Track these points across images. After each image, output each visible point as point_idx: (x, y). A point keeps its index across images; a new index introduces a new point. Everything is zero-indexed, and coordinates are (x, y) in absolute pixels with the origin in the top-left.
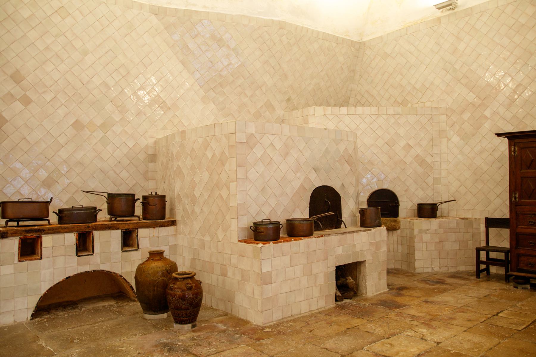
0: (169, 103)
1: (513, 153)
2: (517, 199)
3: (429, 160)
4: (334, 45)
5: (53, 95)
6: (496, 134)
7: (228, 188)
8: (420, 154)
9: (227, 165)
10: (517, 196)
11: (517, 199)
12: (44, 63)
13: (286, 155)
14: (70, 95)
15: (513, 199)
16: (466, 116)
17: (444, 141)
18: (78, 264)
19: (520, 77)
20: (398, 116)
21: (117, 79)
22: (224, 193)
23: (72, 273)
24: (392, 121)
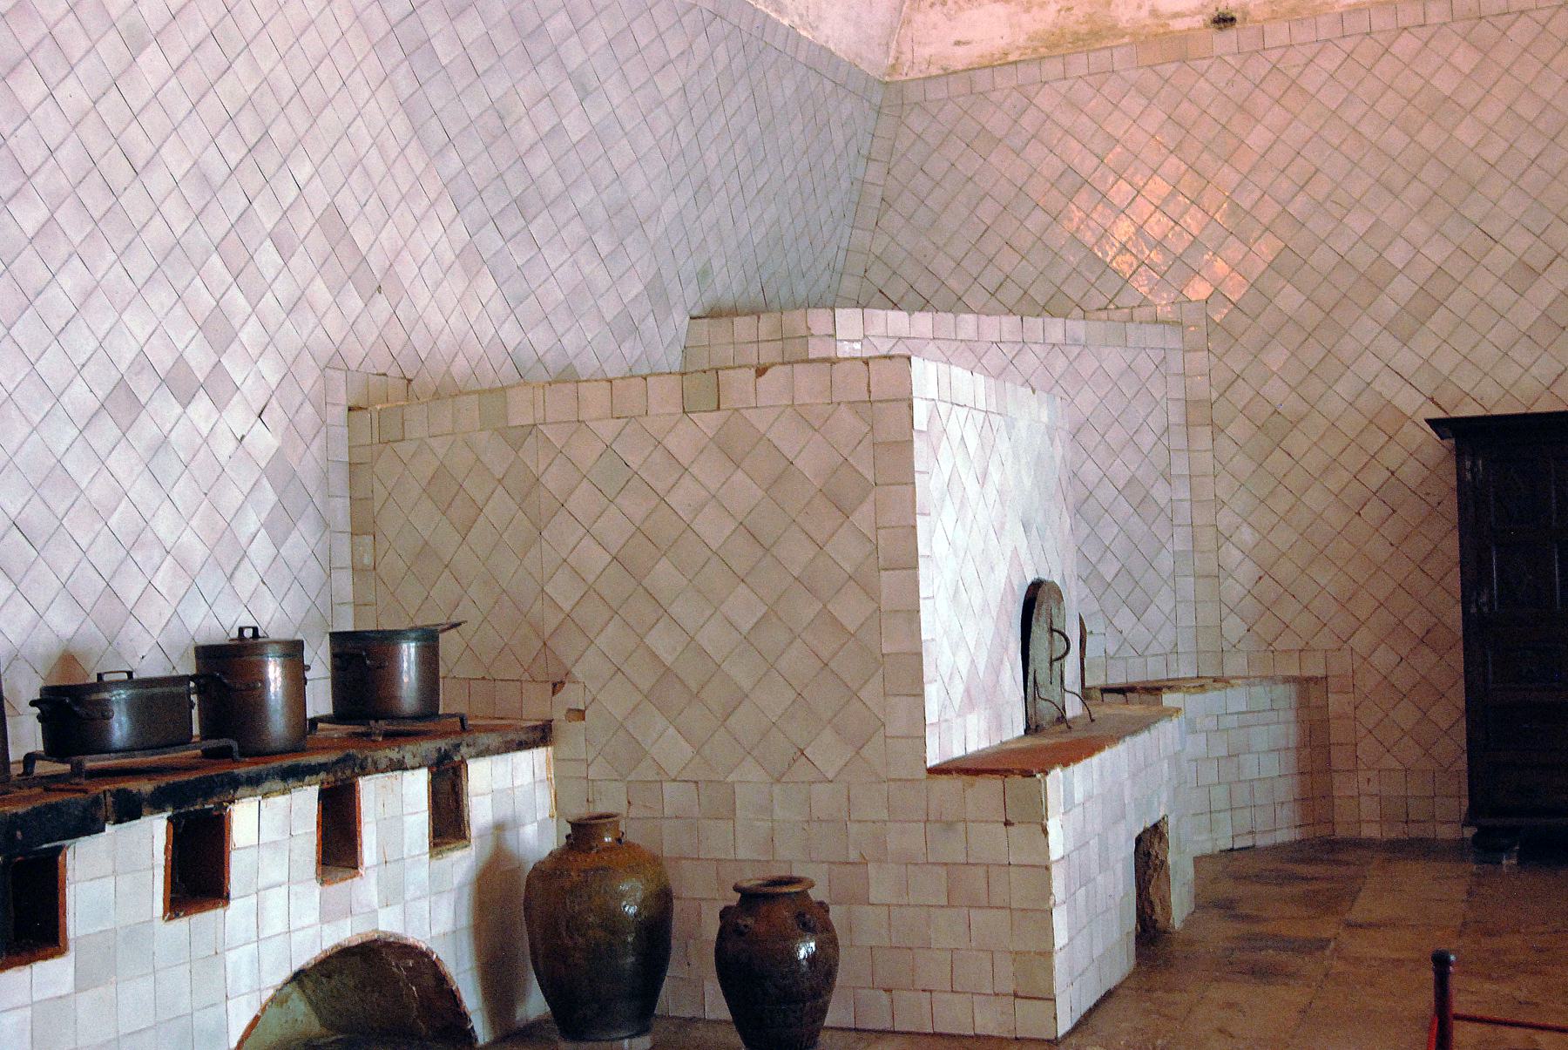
0: (377, 262)
1: (1469, 476)
2: (1485, 609)
3: (1160, 493)
4: (829, 86)
5: (42, 213)
6: (1428, 421)
7: (871, 593)
8: (1139, 474)
9: (867, 507)
10: (1484, 599)
11: (1485, 609)
12: (13, 69)
13: (983, 479)
14: (97, 216)
15: (1473, 610)
16: (1276, 357)
17: (1203, 437)
18: (326, 916)
19: (1437, 252)
20: (1076, 350)
21: (233, 159)
22: (851, 610)
23: (307, 951)
24: (1060, 364)
